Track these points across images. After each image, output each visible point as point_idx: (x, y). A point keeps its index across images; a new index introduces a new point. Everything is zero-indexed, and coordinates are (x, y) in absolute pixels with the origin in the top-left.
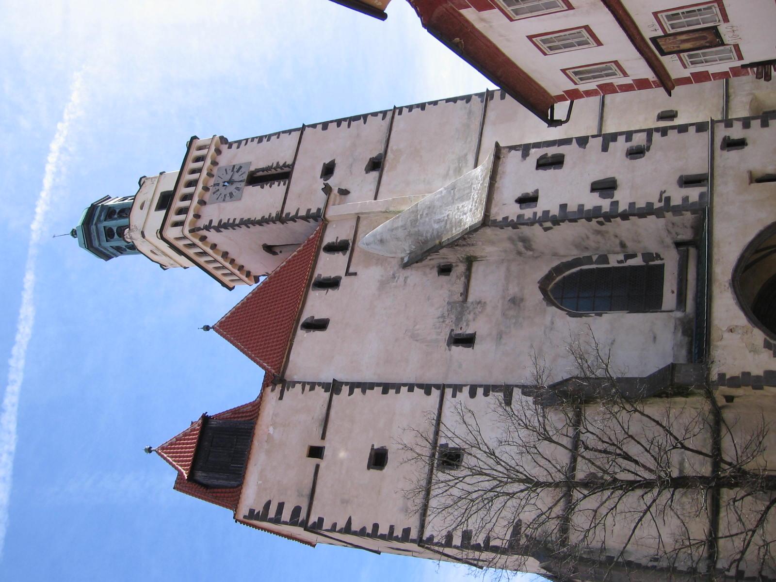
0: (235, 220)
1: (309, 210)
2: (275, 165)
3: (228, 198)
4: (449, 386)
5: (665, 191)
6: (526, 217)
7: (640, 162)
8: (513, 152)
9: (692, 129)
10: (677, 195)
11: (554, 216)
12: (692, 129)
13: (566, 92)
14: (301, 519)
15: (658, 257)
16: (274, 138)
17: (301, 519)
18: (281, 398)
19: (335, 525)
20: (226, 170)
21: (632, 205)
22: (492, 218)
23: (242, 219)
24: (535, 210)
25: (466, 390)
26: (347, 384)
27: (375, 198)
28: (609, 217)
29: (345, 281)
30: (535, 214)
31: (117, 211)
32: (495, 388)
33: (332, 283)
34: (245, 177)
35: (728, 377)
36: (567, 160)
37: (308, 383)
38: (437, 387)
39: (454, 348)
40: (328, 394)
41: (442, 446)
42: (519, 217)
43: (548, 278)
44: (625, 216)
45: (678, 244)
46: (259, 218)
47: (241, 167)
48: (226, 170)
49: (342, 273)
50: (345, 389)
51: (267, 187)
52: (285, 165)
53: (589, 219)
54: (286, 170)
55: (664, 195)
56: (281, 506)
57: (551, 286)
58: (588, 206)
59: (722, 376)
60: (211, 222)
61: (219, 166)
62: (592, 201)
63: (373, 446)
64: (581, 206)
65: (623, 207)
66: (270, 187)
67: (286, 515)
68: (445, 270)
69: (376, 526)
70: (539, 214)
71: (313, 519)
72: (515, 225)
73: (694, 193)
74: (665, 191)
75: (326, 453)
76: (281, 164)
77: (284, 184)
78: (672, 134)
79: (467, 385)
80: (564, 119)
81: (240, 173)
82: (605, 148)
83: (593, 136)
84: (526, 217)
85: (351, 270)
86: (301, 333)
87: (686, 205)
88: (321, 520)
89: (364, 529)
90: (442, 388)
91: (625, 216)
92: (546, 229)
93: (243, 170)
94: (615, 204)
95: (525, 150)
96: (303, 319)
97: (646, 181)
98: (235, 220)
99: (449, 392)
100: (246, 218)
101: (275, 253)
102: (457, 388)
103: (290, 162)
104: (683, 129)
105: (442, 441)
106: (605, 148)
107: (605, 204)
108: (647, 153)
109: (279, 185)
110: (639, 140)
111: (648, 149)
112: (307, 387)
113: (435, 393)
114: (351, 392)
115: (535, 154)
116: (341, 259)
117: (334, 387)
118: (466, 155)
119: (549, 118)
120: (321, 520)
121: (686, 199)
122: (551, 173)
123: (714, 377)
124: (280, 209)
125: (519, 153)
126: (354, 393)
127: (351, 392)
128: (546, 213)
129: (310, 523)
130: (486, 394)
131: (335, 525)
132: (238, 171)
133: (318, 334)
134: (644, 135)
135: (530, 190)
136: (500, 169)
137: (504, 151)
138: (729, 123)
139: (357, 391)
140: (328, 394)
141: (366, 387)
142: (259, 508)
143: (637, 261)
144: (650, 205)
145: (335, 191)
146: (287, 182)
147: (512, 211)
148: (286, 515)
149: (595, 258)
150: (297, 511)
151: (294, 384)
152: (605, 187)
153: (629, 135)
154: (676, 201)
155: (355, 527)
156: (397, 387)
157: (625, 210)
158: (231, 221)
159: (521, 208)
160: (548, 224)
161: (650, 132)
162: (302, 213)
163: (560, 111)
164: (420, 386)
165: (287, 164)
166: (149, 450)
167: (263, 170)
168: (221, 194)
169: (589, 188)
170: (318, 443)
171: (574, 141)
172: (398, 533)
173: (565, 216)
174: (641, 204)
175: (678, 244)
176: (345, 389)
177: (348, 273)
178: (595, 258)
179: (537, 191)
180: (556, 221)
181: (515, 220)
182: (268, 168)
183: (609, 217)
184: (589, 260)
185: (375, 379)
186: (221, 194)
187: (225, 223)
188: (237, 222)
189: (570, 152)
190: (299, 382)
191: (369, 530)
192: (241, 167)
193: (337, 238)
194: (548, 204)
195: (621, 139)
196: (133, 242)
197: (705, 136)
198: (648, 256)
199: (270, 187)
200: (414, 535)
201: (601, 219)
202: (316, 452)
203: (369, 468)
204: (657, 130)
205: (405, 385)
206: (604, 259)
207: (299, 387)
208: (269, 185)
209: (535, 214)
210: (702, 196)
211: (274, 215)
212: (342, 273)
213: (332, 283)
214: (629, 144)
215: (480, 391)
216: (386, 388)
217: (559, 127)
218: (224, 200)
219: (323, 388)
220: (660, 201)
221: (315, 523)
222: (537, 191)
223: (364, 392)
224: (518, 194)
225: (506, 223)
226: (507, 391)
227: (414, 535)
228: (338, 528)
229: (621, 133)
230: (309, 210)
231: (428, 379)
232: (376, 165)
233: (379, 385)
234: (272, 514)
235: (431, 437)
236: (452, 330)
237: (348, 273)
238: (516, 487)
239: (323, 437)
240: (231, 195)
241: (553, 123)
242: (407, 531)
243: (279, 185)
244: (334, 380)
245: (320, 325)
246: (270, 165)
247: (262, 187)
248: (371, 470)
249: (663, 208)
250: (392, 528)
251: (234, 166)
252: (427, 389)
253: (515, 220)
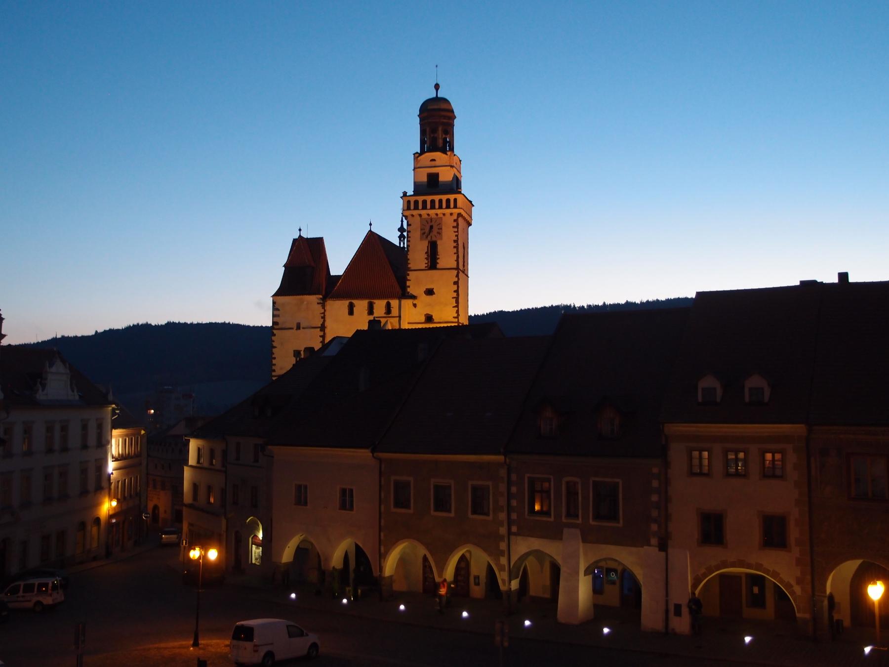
16: (455, 250)
34: (434, 239)
50: (322, 334)
56: (278, 316)
71: (275, 332)
86: (347, 302)
96: (354, 301)
117: (323, 328)
133: (347, 311)
151: (324, 307)
155: (274, 350)
166: (300, 230)
202: (298, 327)
242: (274, 371)
245: (351, 312)
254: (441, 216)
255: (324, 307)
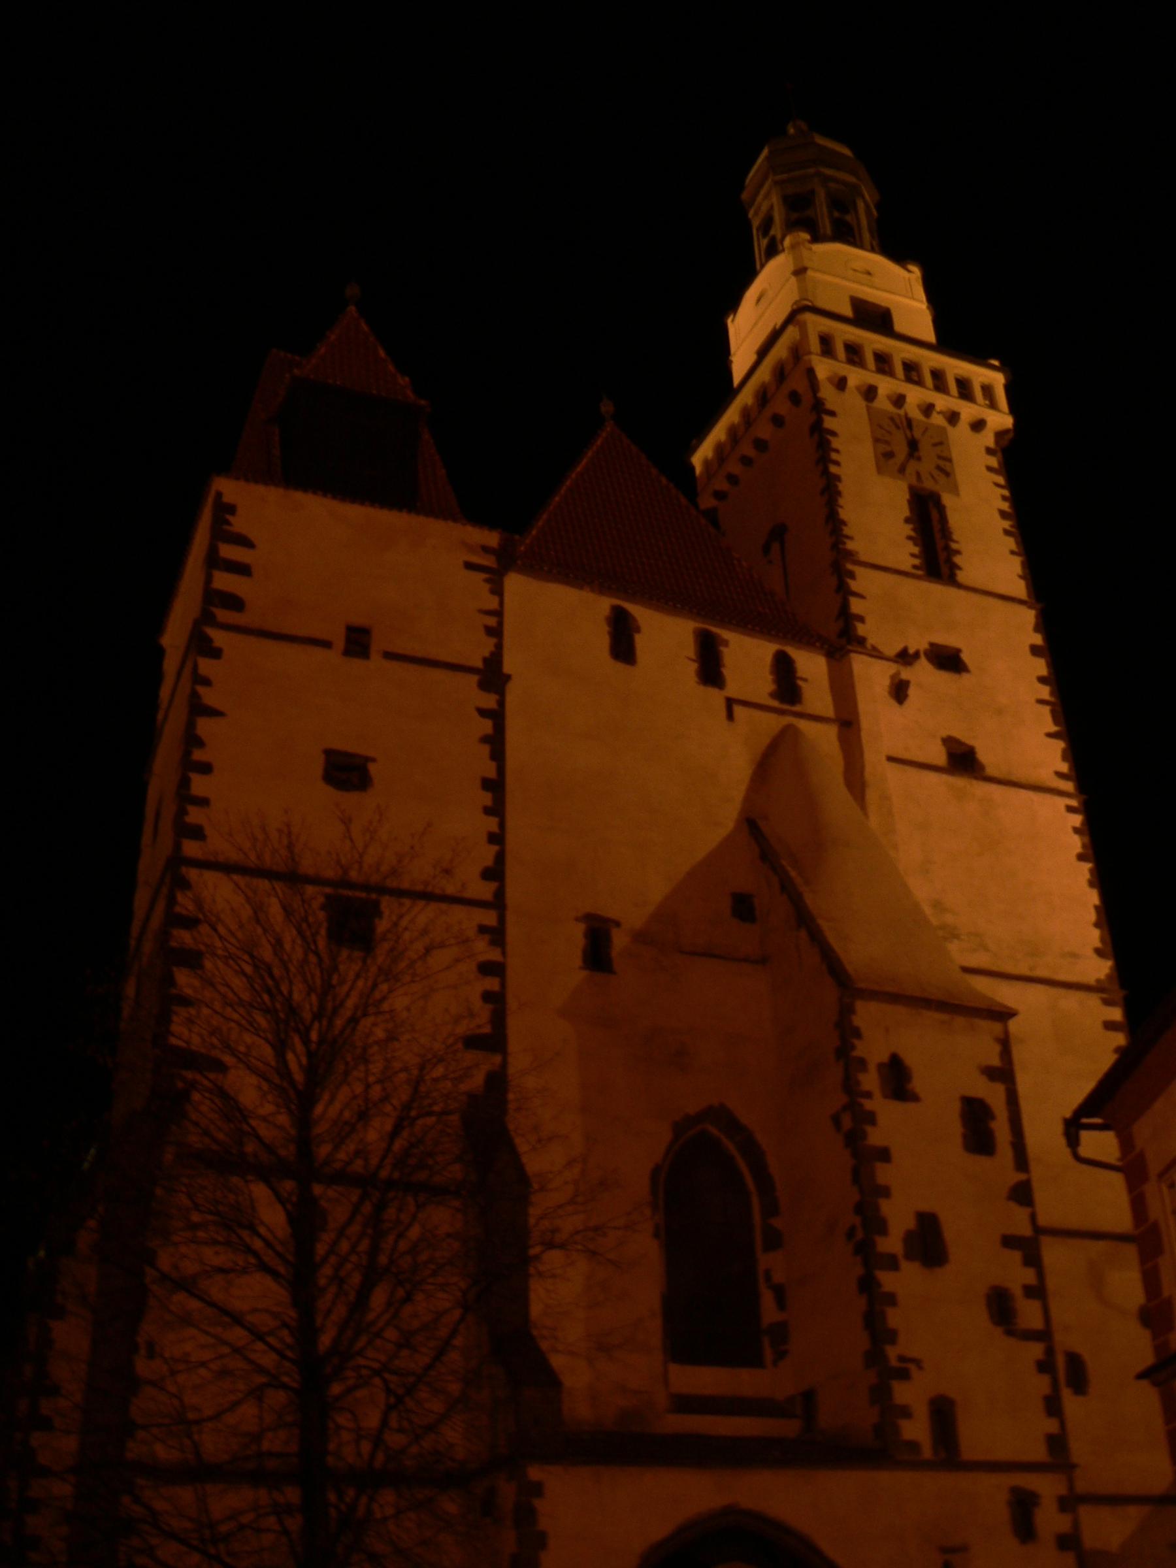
0: (837, 463)
1: (861, 619)
2: (954, 546)
3: (883, 448)
4: (502, 919)
5: (920, 1368)
6: (862, 1077)
7: (980, 1316)
8: (997, 1048)
9: (1051, 1426)
10: (910, 1393)
11: (864, 1135)
12: (1051, 1426)
13: (1141, 1156)
14: (214, 610)
15: (780, 1355)
17: (214, 610)
18: (469, 566)
19: (207, 682)
20: (941, 443)
21: (891, 1299)
22: (859, 1005)
23: (838, 478)
24: (877, 1093)
25: (494, 955)
26: (501, 703)
27: (891, 759)
28: (865, 1250)
29: (715, 697)
30: (869, 1095)
31: (848, 218)
32: (499, 1019)
33: (710, 669)
34: (928, 484)
35: (536, 1502)
36: (983, 1161)
37: (501, 624)
38: (500, 894)
39: (581, 927)
40: (479, 664)
41: (377, 904)
42: (862, 1064)
43: (732, 1125)
44: (867, 1285)
45: (808, 1397)
46: (843, 514)
47: (947, 474)
48: (941, 443)
49: (733, 688)
50: (489, 701)
51: (908, 530)
52: (954, 567)
53: (859, 1209)
54: (945, 569)
55: (912, 1367)
56: (243, 570)
57: (713, 1130)
58: (887, 1207)
59: (537, 1489)
60: (832, 414)
61: (949, 428)
62: (899, 1216)
63: (374, 760)
64: (886, 1192)
65: (888, 1280)
66: (909, 538)
67: (224, 581)
68: (743, 907)
69: (206, 768)
70: (868, 1104)
71: (219, 638)
72: (844, 1051)
73: (917, 1429)
74: (920, 1368)
75: (357, 664)
76: (957, 560)
77: (915, 567)
78: (1042, 1384)
79: (504, 953)
80: (1083, 1151)
81: (936, 473)
82: (1009, 1242)
83: (1033, 1218)
84: (862, 1077)
85: (738, 710)
86: (604, 604)
87: (893, 1412)
88: (216, 653)
89: (200, 743)
90: (498, 903)
91: (867, 1285)
92: (836, 1120)
93: (942, 479)
94: (892, 1263)
95: (1003, 1073)
96: (636, 610)
97: (942, 1330)
98: (837, 463)
99: (489, 918)
100: (841, 487)
101: (766, 549)
102: (496, 935)
103: (961, 577)
104: (1053, 1406)
105: (386, 903)
106: (1009, 1242)
107: (892, 1243)
108: (999, 1331)
109: (913, 555)
110: (1030, 1314)
111: (1010, 1333)
112: (492, 621)
113: (485, 890)
114: (483, 712)
115: (995, 1096)
116: (762, 686)
117: (492, 676)
118: (986, 949)
119: (1085, 1120)
120: (216, 653)
121: (905, 1412)
122: (956, 1128)
123: (535, 1473)
124: (863, 557)
125: (996, 1061)
126: (481, 719)
127: (483, 712)
128: (871, 1118)
129: (212, 633)
130: (487, 996)
131: (207, 682)
132: (939, 468)
133: (602, 641)
134: (1037, 1323)
135: (918, 1084)
136: (960, 1021)
137: (997, 1027)
138: (1068, 1503)
139: (487, 726)
140: (479, 664)
141: (496, 743)
142: (238, 524)
143: (769, 1312)
144: (892, 1336)
145: (906, 674)
146: (920, 573)
147: (874, 1049)
148: (224, 581)
149: (777, 1222)
150: (235, 603)
152: (928, 1242)
153: (1037, 1292)
154: (903, 1393)
155: (205, 726)
156: (496, 809)
157: (879, 1285)
158: (834, 456)
159: (880, 1066)
160: (847, 1122)
161: (1044, 1335)
162: (856, 606)
163: (1100, 1143)
164: (500, 858)
165: (958, 572)
167: (943, 519)
168: (889, 432)
169: (924, 1207)
170: (376, 646)
171: (1022, 1177)
172: (195, 815)
173: (866, 1159)
174: (894, 1318)
175: (808, 1397)
176: (489, 701)
177: (730, 702)
178: (777, 1222)
179: (915, 1098)
180: (854, 1139)
181: (855, 1053)
182: (946, 534)
183: (865, 1250)
184: (771, 1209)
185: (511, 764)
186: (889, 432)
187: (829, 442)
188: (833, 469)
189: (1000, 1168)
190: (501, 603)
191: (198, 755)
192: (947, 474)
193: (805, 680)
194: (890, 1122)
195: (1029, 1276)
196: (783, 250)
197: (1039, 1453)
198: (780, 1333)
199: (909, 538)
200: (191, 848)
201: (860, 1235)
202: (358, 642)
203: (329, 753)
204: (1050, 1351)
205: (502, 825)
206: (774, 1241)
207: (493, 603)
208: (912, 534)
209: (869, 1095)
210: (914, 1446)
211: (850, 545)
212: (733, 688)
213: (710, 669)
214: (1018, 1292)
215: (492, 983)
216: (495, 786)
217: (1062, 1141)
218: (876, 440)
219: (492, 654)
220: (902, 1359)
221: (210, 640)
222: (915, 1098)
223: (485, 739)
224: (911, 1059)
225: (847, 1033)
226: (493, 1040)
227: (191, 848)
228: (201, 689)
229: (1041, 1275)
230: (861, 619)
231: (513, 872)
232: (962, 760)
233: (501, 770)
234: (228, 551)
235: (391, 883)
236: (618, 924)
237: (730, 702)
238: (295, 1061)
239: (389, 656)
240: (889, 455)
241: (1073, 1128)
242: (197, 833)
243: (913, 555)
244: (508, 677)
245: (623, 645)
246: (955, 537)
247: (907, 521)
248: (323, 757)
249: (884, 1368)
250: (204, 802)
251: (950, 460)
252: (495, 873)
253: (855, 1053)
254: (938, 420)
255: (498, 590)
